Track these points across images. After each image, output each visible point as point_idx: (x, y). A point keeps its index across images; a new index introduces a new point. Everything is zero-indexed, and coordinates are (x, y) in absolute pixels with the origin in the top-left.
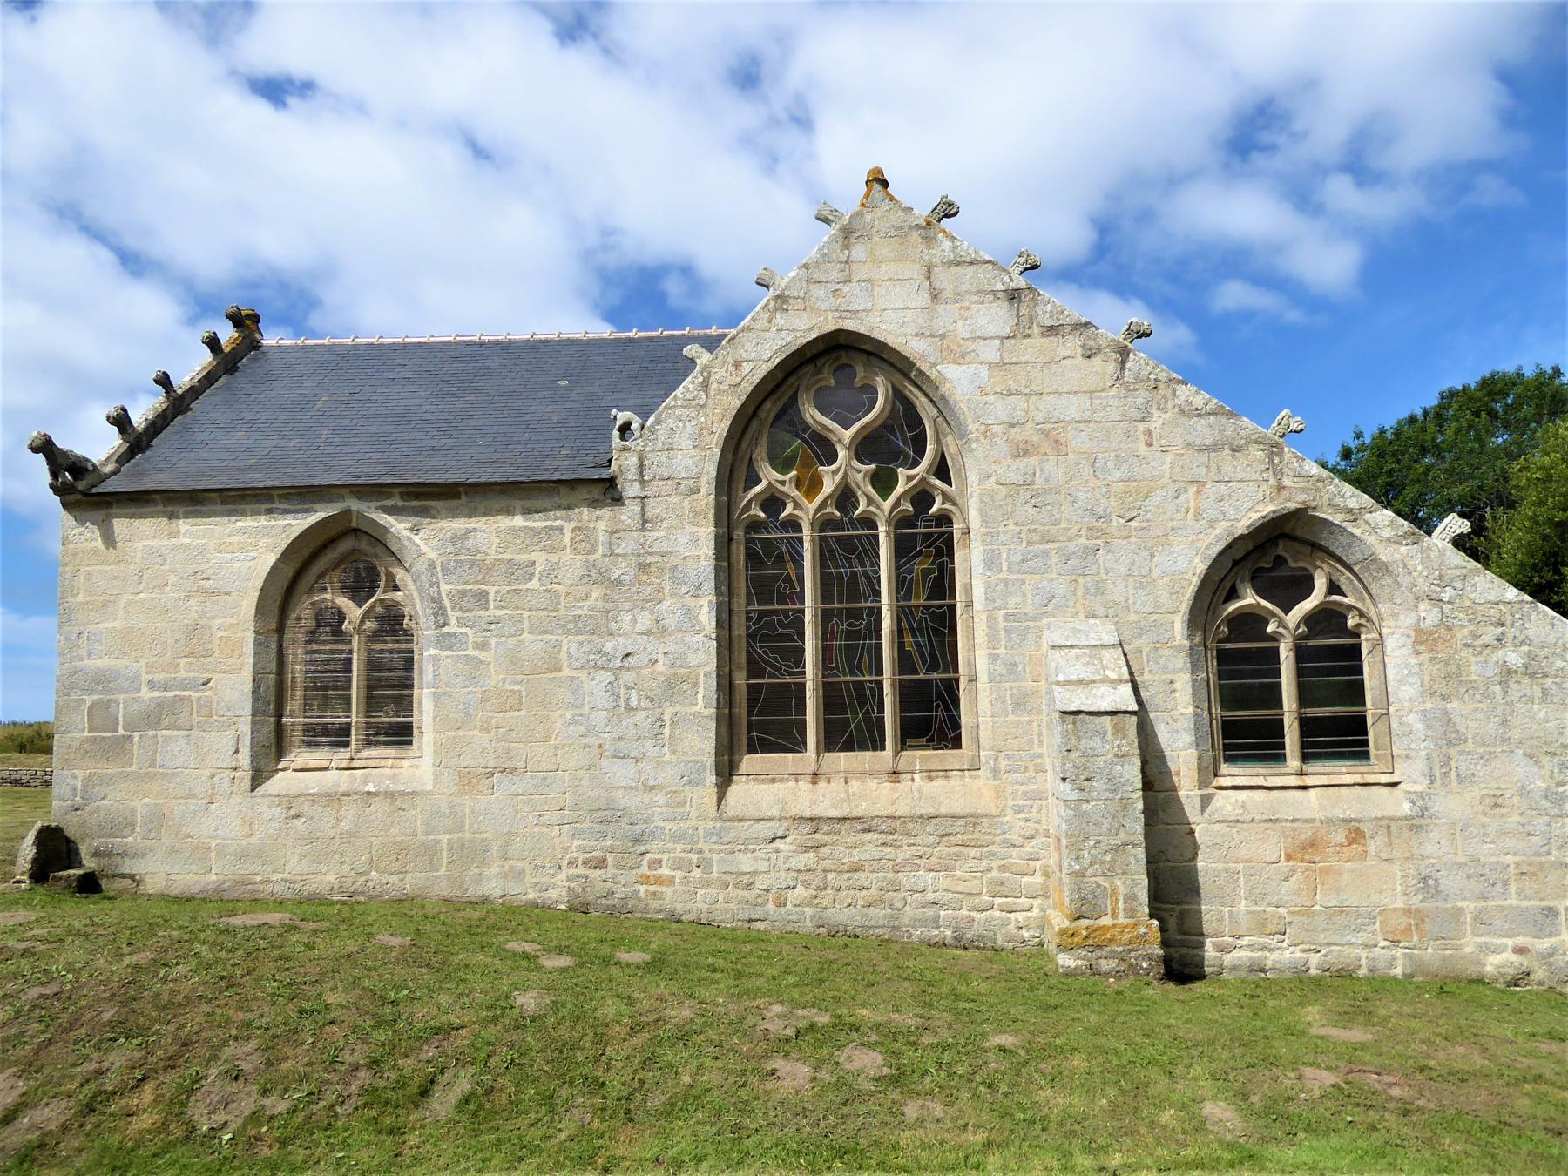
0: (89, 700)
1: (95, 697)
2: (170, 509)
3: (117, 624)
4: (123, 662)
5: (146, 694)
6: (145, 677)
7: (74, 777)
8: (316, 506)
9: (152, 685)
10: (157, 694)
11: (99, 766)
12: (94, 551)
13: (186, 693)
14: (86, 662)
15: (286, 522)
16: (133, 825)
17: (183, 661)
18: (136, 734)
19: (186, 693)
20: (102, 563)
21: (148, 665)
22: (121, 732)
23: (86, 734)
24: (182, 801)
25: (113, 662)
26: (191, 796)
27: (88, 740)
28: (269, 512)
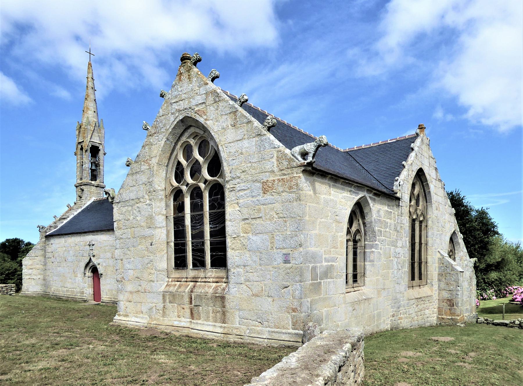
0: (311, 265)
1: (312, 265)
2: (329, 182)
3: (317, 232)
4: (318, 249)
5: (325, 264)
6: (324, 256)
7: (308, 302)
8: (360, 192)
9: (327, 260)
10: (326, 264)
11: (314, 296)
12: (310, 195)
13: (333, 263)
14: (309, 248)
15: (353, 196)
16: (322, 320)
17: (332, 250)
18: (322, 281)
19: (333, 263)
20: (313, 203)
21: (325, 251)
22: (319, 280)
23: (310, 282)
24: (333, 308)
25: (316, 249)
26: (335, 306)
27: (312, 284)
28: (350, 191)
